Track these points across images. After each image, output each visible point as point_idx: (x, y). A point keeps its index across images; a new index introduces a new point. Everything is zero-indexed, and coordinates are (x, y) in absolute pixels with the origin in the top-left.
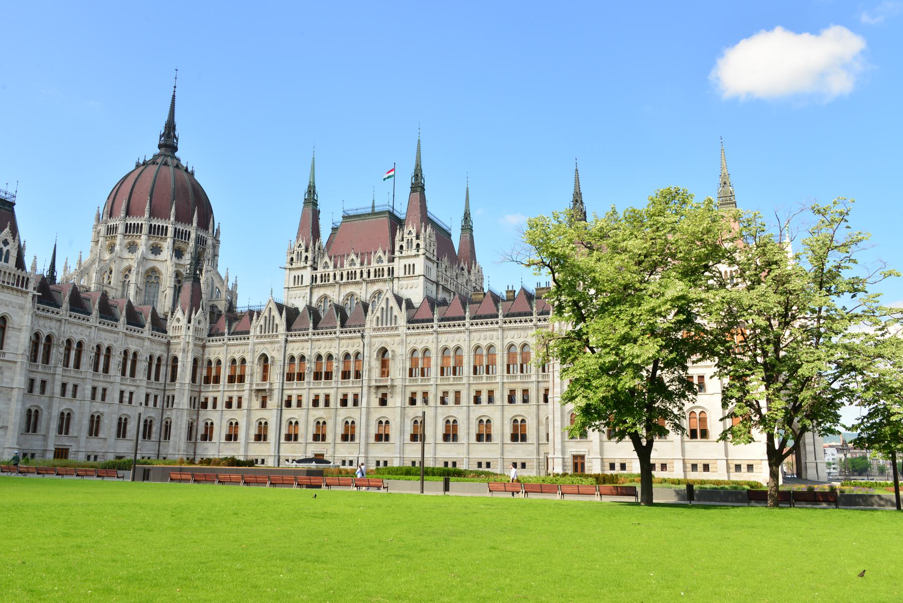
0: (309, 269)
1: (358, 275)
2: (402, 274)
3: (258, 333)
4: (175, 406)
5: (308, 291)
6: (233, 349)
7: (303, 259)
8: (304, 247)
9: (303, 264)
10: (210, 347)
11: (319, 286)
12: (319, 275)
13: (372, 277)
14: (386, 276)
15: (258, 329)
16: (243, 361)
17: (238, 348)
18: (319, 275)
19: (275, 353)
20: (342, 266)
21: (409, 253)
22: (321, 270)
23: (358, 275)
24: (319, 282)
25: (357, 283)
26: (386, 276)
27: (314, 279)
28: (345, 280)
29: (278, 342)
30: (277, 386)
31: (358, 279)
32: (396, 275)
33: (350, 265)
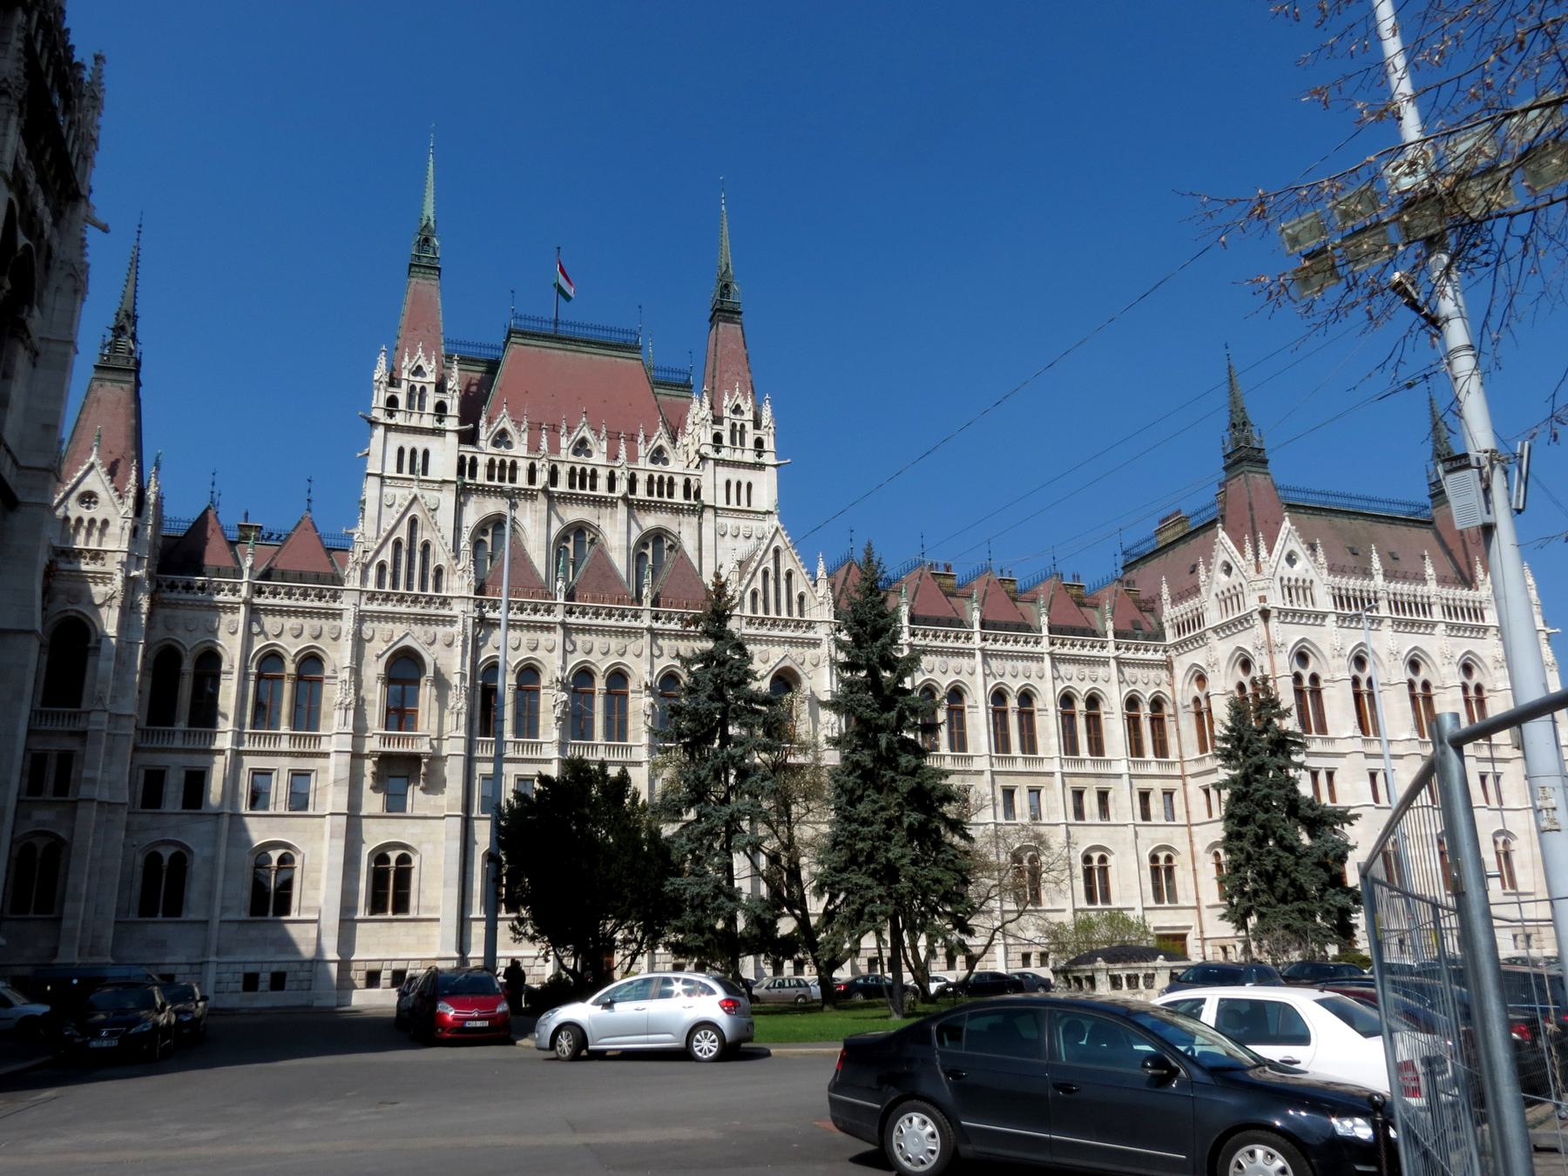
0: (452, 439)
1: (602, 483)
2: (721, 503)
3: (371, 586)
4: (84, 791)
5: (448, 498)
6: (270, 623)
7: (430, 406)
8: (431, 378)
9: (428, 422)
10: (176, 605)
11: (483, 491)
12: (482, 460)
13: (641, 493)
14: (679, 497)
15: (373, 572)
16: (311, 661)
17: (291, 623)
18: (482, 460)
19: (447, 656)
20: (555, 448)
21: (737, 456)
22: (485, 452)
23: (602, 483)
24: (481, 477)
25: (599, 502)
26: (679, 497)
27: (465, 466)
28: (562, 486)
29: (451, 621)
30: (454, 747)
31: (602, 489)
32: (707, 497)
33: (576, 452)
